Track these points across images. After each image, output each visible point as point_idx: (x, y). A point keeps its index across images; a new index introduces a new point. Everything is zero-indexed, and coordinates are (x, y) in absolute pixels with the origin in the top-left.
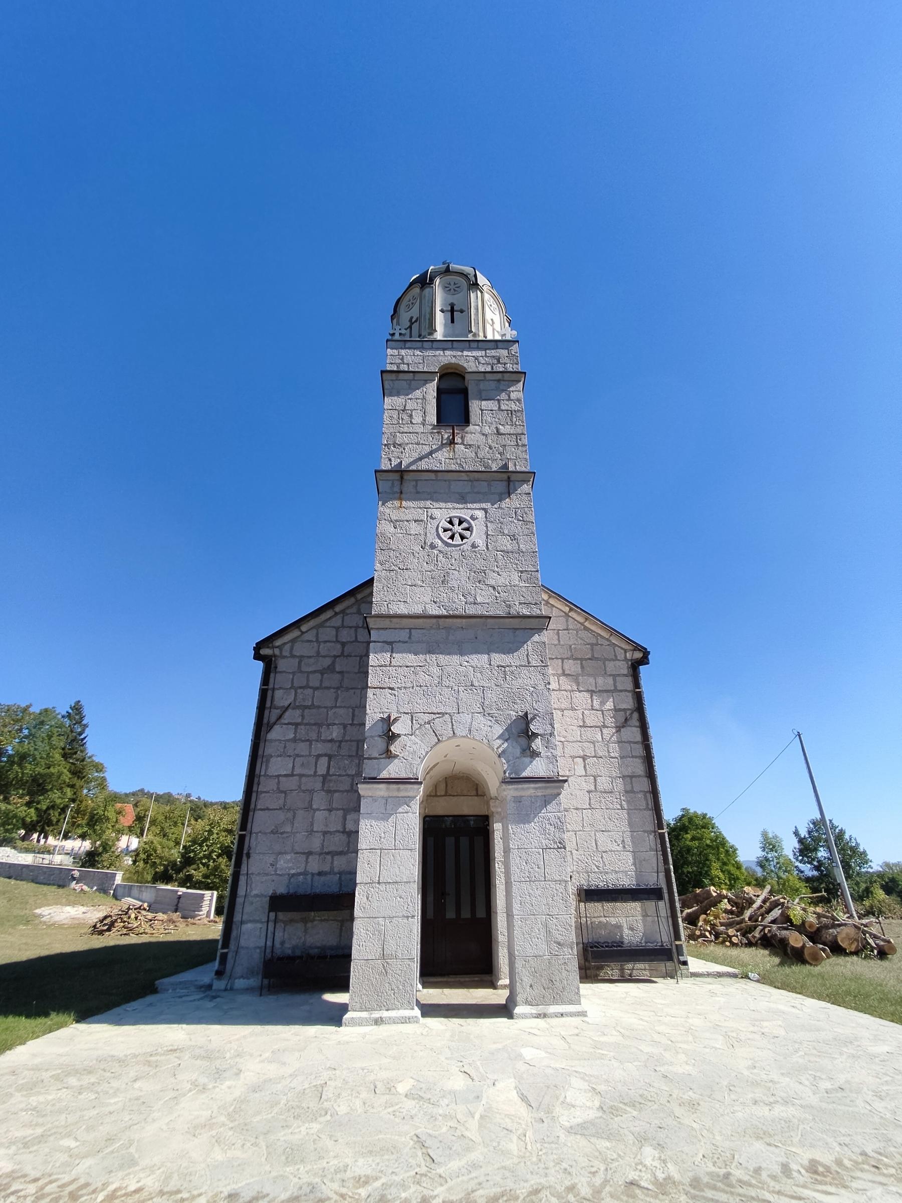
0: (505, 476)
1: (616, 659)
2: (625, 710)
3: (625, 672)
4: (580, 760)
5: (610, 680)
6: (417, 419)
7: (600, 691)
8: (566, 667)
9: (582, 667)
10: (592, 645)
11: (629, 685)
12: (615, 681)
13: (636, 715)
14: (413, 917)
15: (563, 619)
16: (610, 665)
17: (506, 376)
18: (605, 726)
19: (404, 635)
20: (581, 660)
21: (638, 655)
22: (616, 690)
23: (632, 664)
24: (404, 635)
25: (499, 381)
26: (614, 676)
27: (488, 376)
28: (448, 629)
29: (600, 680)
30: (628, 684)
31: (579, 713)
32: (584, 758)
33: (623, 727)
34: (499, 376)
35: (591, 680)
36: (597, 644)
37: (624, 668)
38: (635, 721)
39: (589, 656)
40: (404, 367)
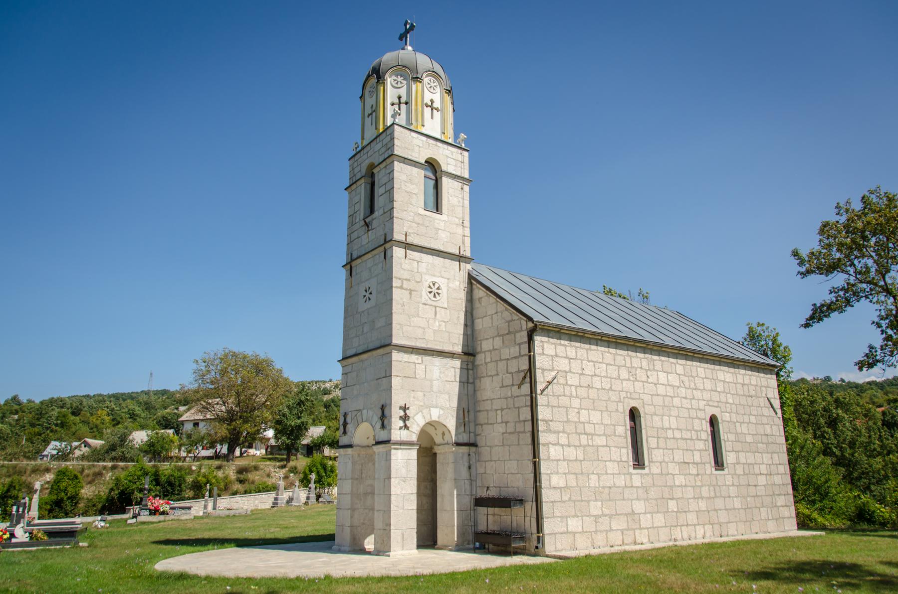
0: (382, 249)
1: (522, 330)
3: (526, 339)
4: (499, 412)
10: (509, 322)
16: (518, 335)
18: (513, 385)
20: (503, 335)
21: (531, 325)
26: (520, 344)
28: (362, 361)
29: (512, 350)
32: (502, 410)
35: (507, 351)
36: (513, 320)
38: (528, 379)
39: (507, 332)
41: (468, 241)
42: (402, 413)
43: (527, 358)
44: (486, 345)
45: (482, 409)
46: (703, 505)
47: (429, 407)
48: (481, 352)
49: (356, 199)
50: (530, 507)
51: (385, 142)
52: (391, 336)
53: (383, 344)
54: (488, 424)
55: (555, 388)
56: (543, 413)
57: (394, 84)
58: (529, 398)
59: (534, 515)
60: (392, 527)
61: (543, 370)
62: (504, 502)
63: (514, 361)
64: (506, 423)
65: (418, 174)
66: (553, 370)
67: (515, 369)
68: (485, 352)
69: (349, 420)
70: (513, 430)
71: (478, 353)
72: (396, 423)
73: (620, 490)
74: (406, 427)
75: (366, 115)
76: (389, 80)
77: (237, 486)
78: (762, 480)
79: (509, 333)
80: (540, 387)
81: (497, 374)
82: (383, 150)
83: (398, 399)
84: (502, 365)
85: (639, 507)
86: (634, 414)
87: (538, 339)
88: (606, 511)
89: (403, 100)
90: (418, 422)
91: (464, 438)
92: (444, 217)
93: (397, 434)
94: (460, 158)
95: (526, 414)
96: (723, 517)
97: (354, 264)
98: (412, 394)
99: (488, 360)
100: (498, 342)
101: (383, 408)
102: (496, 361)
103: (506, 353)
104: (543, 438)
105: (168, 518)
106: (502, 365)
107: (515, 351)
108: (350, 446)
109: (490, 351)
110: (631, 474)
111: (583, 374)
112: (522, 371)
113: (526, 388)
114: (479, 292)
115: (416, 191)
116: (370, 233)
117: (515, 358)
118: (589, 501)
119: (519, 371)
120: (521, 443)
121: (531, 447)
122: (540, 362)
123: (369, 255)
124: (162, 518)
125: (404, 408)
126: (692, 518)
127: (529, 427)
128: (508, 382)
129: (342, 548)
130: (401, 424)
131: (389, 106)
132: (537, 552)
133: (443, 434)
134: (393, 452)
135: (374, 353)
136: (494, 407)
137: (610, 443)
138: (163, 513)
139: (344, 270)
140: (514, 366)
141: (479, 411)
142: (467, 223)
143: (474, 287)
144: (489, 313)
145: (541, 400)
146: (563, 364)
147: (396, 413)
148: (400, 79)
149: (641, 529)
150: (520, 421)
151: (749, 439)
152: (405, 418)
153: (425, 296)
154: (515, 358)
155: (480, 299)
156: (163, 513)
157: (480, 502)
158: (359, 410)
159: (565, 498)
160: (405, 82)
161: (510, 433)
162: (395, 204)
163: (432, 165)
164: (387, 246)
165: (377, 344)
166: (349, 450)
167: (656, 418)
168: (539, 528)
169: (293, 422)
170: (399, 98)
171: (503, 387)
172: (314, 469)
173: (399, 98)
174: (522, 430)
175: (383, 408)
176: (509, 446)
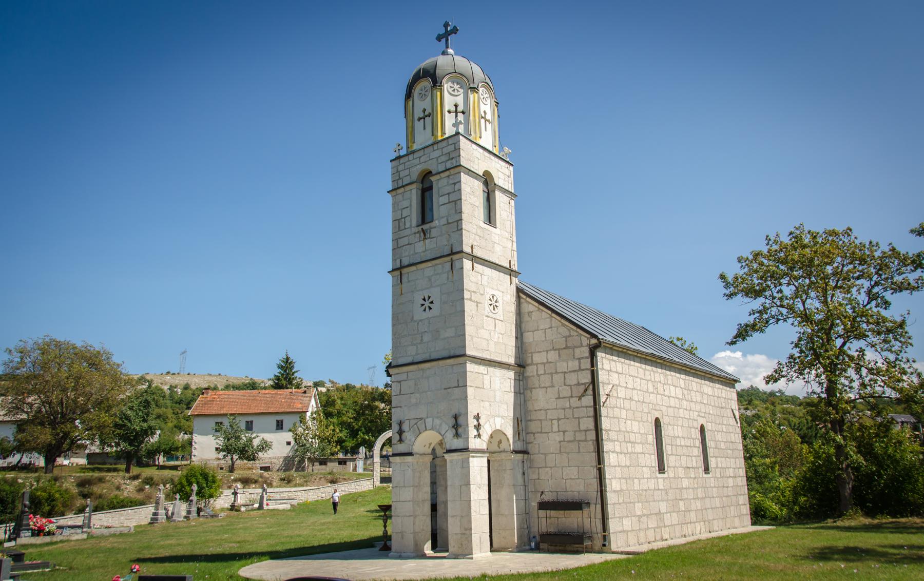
0: (449, 258)
1: (582, 346)
2: (585, 384)
3: (587, 354)
4: (555, 422)
5: (577, 362)
6: (408, 225)
7: (570, 372)
8: (549, 357)
9: (559, 356)
10: (566, 337)
11: (589, 366)
12: (580, 363)
13: (591, 387)
14: (453, 516)
15: (548, 320)
16: (577, 351)
17: (452, 171)
18: (572, 397)
19: (404, 376)
20: (559, 350)
21: (594, 341)
22: (580, 369)
23: (590, 349)
24: (404, 376)
25: (448, 176)
26: (579, 359)
27: (443, 175)
28: (422, 369)
29: (570, 364)
30: (586, 364)
31: (556, 389)
33: (583, 395)
34: (447, 173)
35: (565, 364)
36: (570, 336)
37: (586, 353)
38: (590, 392)
40: (400, 184)
41: (515, 253)
42: (476, 423)
43: (589, 372)
44: (537, 358)
45: (533, 418)
46: (699, 505)
47: (494, 416)
48: (532, 364)
49: (406, 203)
50: (596, 509)
51: (445, 151)
52: (464, 347)
53: (452, 354)
54: (541, 432)
55: (612, 401)
56: (605, 424)
57: (450, 90)
58: (592, 409)
59: (599, 515)
60: (473, 532)
61: (604, 383)
62: (577, 505)
63: (573, 374)
64: (564, 432)
65: (478, 186)
66: (609, 384)
67: (575, 382)
68: (537, 364)
69: (405, 427)
70: (572, 439)
71: (528, 365)
72: (472, 432)
73: (651, 492)
74: (479, 435)
75: (416, 118)
76: (447, 86)
77: (79, 502)
78: (731, 482)
79: (566, 348)
80: (603, 399)
81: (553, 386)
82: (444, 158)
83: (472, 410)
84: (558, 378)
85: (663, 507)
86: (657, 423)
87: (600, 355)
88: (645, 512)
89: (460, 108)
90: (486, 431)
91: (519, 447)
92: (497, 231)
93: (474, 443)
94: (506, 171)
95: (589, 423)
96: (710, 515)
97: (404, 271)
98: (482, 404)
99: (541, 372)
100: (553, 356)
101: (456, 417)
102: (551, 374)
103: (562, 366)
104: (607, 446)
105: (55, 539)
106: (558, 378)
107: (574, 365)
108: (410, 454)
109: (544, 364)
110: (657, 478)
111: (626, 388)
112: (582, 384)
113: (588, 400)
114: (530, 306)
115: (477, 204)
116: (427, 241)
117: (574, 371)
118: (634, 503)
119: (578, 384)
120: (581, 450)
121: (594, 455)
122: (602, 376)
123: (429, 264)
124: (47, 539)
125: (477, 417)
126: (693, 515)
127: (592, 436)
128: (566, 392)
129: (403, 554)
130: (475, 433)
131: (447, 114)
132: (604, 547)
133: (500, 442)
134: (471, 459)
135: (441, 362)
136: (549, 417)
137: (645, 451)
138: (50, 533)
139: (390, 277)
140: (572, 379)
141: (530, 421)
142: (514, 238)
143: (522, 300)
144: (542, 327)
145: (603, 411)
146: (614, 379)
147: (472, 422)
148: (456, 86)
149: (665, 527)
150: (580, 431)
151: (723, 446)
152: (478, 427)
153: (488, 309)
154: (574, 371)
155: (530, 313)
156: (50, 533)
157: (543, 506)
158: (421, 419)
159: (621, 501)
160: (461, 91)
161: (569, 442)
162: (464, 216)
163: (487, 180)
164: (455, 257)
165: (445, 354)
166: (409, 458)
167: (670, 428)
168: (605, 528)
169: (137, 425)
170: (456, 106)
171: (559, 398)
172: (193, 480)
173: (456, 106)
174: (583, 438)
175: (456, 417)
176: (568, 453)
